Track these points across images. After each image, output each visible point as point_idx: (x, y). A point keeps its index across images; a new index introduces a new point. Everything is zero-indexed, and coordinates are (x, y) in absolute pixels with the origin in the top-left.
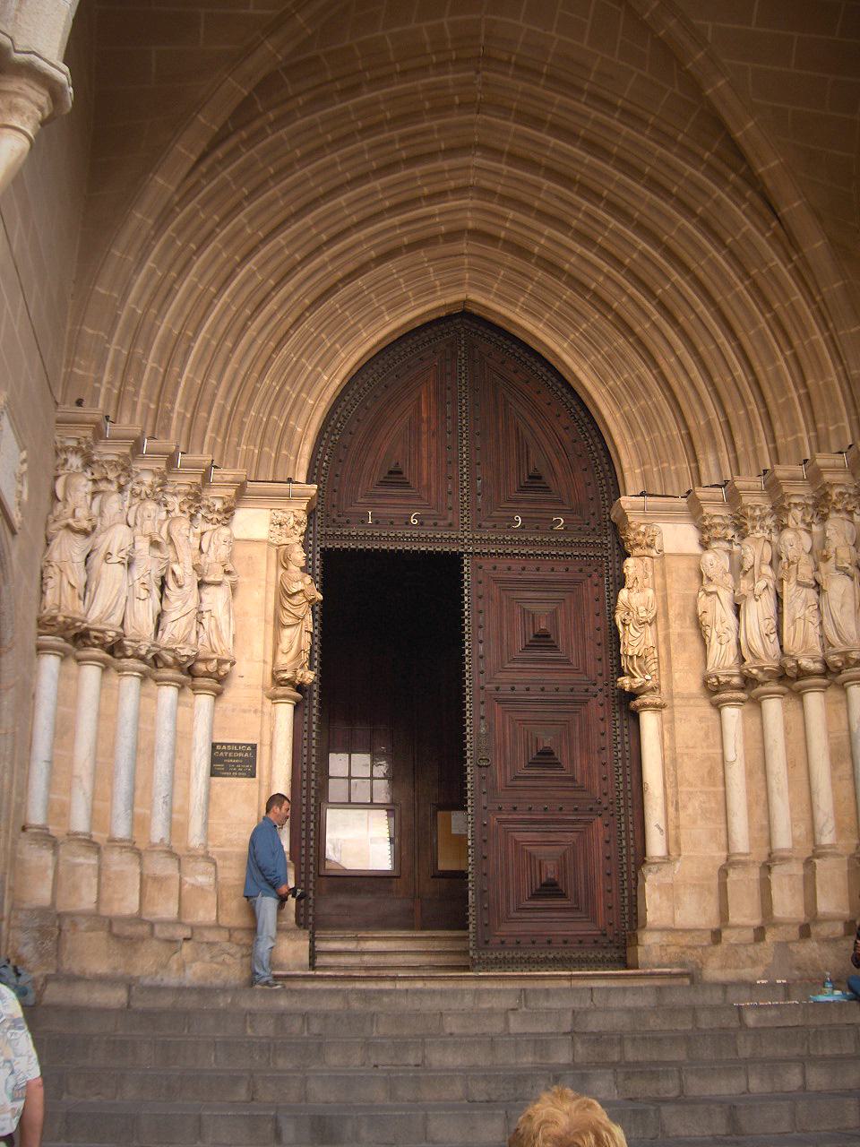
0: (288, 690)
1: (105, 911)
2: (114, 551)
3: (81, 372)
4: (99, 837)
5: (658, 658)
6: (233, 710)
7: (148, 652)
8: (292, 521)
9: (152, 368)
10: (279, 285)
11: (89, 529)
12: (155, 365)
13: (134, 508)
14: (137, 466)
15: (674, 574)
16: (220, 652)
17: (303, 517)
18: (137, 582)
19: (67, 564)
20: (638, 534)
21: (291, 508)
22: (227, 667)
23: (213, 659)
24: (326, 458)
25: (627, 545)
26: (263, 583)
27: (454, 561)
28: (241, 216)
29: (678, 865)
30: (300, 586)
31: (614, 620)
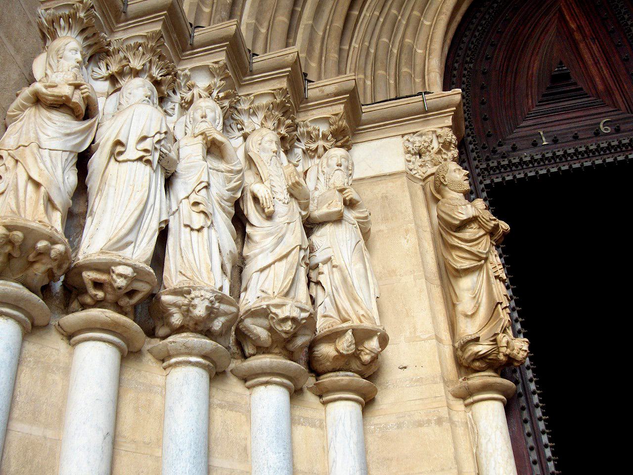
0: (488, 377)
6: (399, 426)
7: (212, 313)
8: (436, 145)
14: (184, 68)
17: (451, 137)
18: (185, 202)
19: (27, 150)
21: (431, 128)
22: (374, 344)
23: (343, 332)
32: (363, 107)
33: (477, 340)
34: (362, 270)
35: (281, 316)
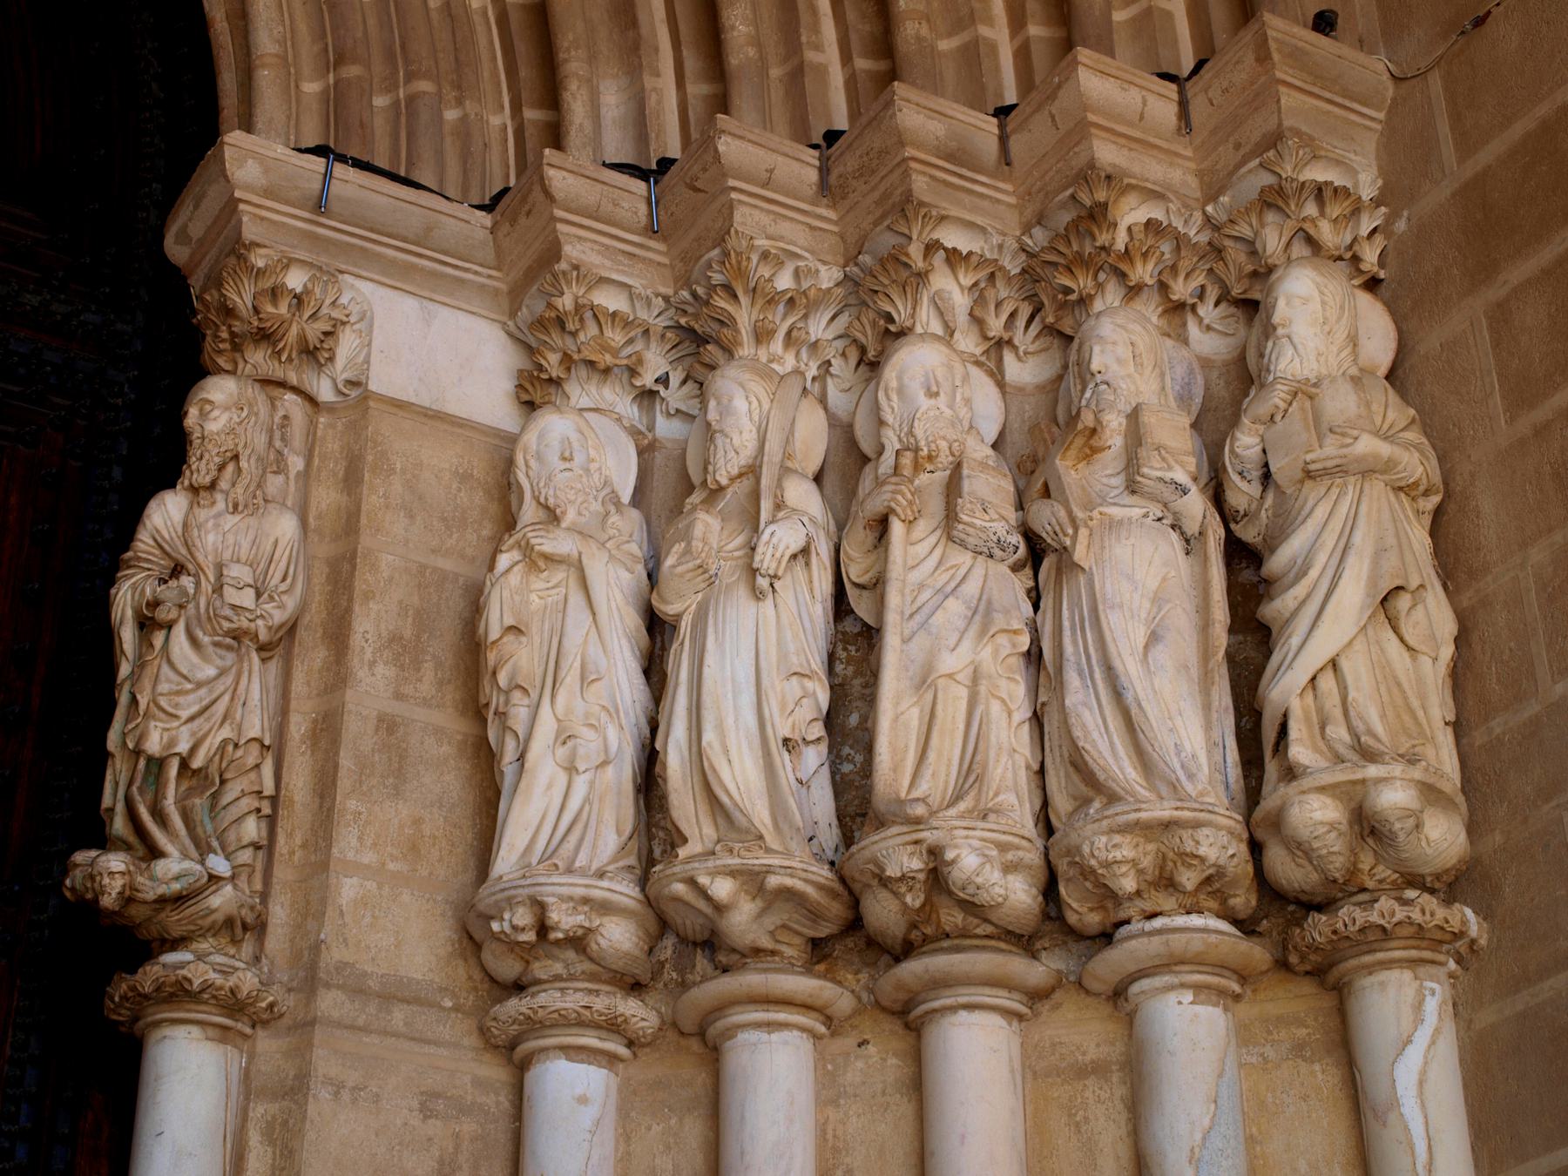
5: (274, 800)
15: (397, 486)
31: (105, 605)
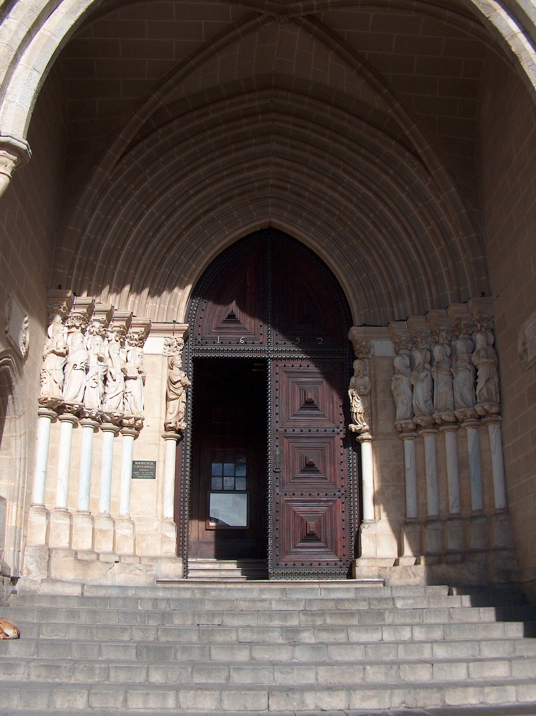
1: (74, 547)
2: (78, 364)
3: (61, 271)
4: (71, 509)
6: (144, 444)
7: (97, 415)
8: (175, 344)
9: (100, 266)
10: (167, 218)
11: (65, 352)
12: (101, 264)
13: (90, 340)
16: (136, 414)
20: (361, 347)
22: (140, 421)
24: (195, 309)
25: (356, 353)
26: (160, 377)
27: (264, 361)
28: (146, 183)
29: (379, 524)
30: (179, 378)
32: (152, 324)
33: (171, 423)
34: (140, 396)
35: (115, 415)
